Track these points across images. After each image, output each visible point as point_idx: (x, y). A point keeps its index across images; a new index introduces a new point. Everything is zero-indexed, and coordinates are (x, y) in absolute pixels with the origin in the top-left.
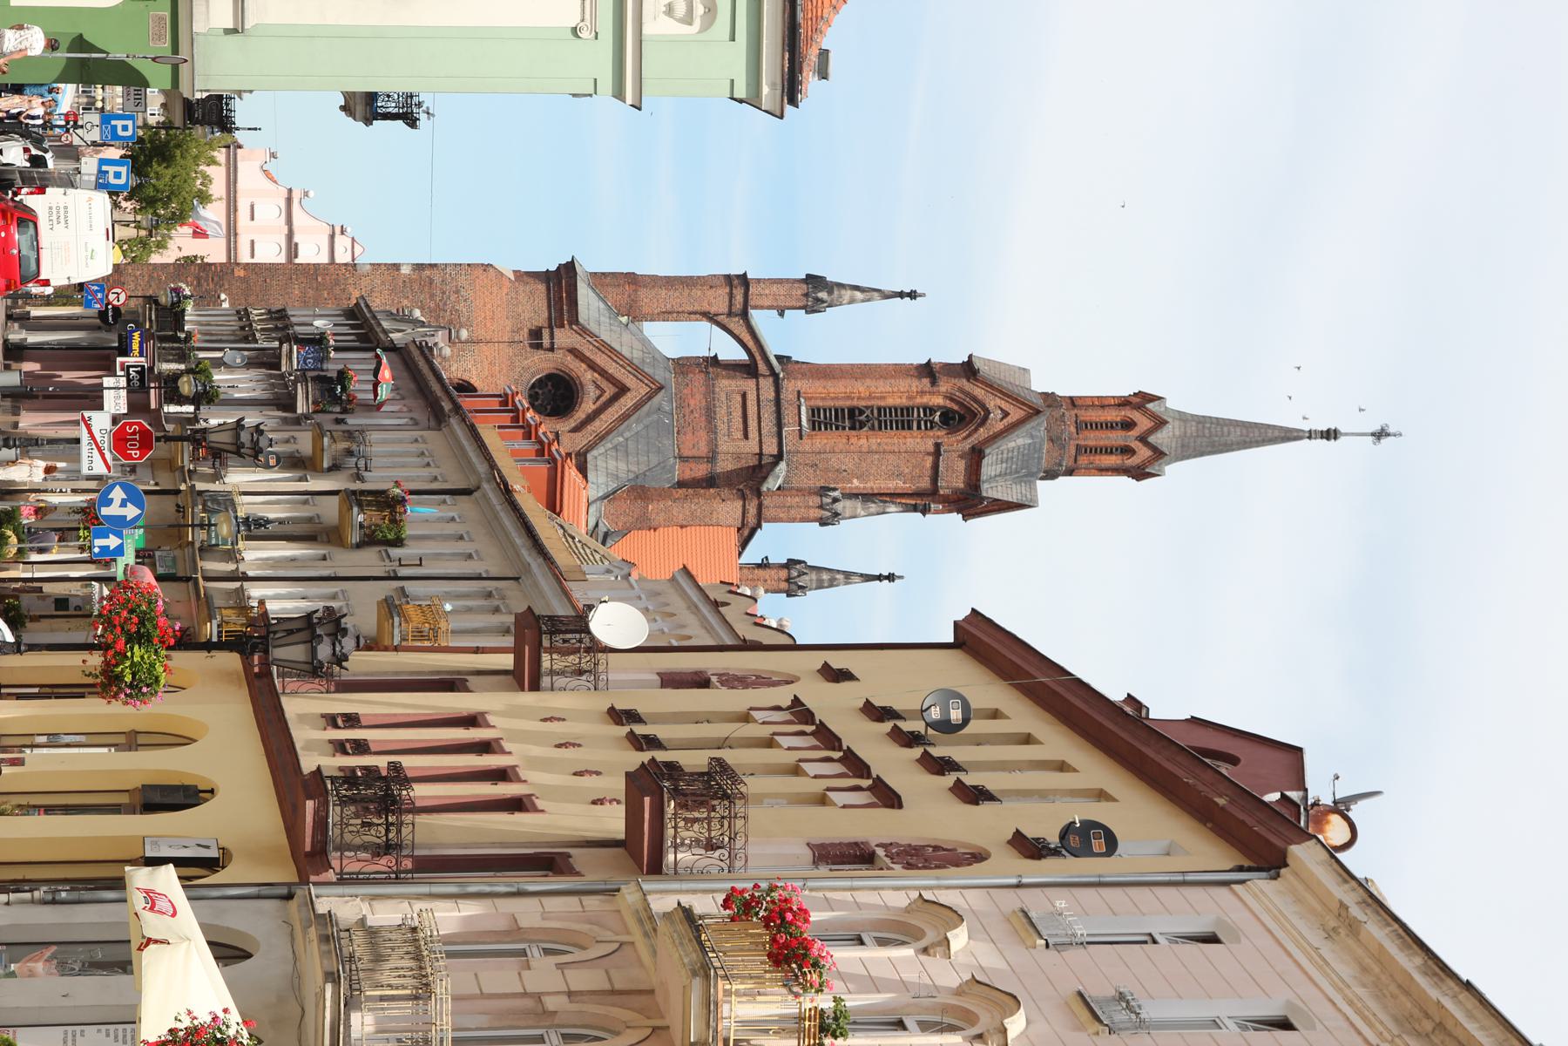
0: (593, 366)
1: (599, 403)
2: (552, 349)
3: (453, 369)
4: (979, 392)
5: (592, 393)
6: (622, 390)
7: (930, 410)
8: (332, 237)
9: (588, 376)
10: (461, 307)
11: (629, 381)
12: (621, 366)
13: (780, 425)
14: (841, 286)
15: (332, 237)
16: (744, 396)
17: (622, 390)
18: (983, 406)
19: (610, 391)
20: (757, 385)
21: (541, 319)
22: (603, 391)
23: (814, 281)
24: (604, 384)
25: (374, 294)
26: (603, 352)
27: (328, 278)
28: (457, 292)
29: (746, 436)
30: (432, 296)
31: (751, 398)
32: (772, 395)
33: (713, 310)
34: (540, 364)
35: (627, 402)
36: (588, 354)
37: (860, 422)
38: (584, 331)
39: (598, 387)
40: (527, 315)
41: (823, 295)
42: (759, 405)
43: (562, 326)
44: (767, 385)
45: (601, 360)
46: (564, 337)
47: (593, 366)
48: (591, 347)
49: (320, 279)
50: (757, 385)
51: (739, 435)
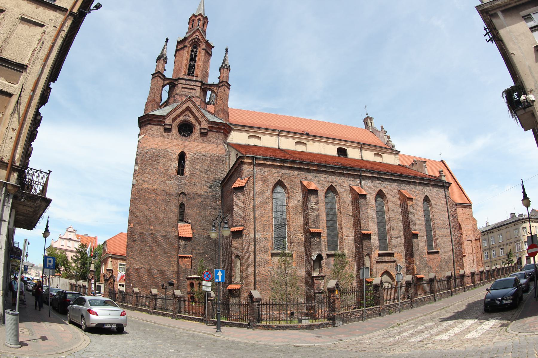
0: (179, 116)
1: (191, 116)
2: (171, 125)
3: (174, 157)
4: (190, 39)
5: (187, 118)
6: (188, 109)
7: (192, 51)
8: (68, 231)
9: (182, 118)
10: (152, 152)
11: (186, 106)
12: (180, 107)
13: (193, 81)
14: (162, 53)
15: (68, 231)
16: (183, 88)
17: (188, 109)
18: (194, 39)
19: (188, 112)
20: (180, 84)
21: (161, 129)
22: (187, 114)
23: (159, 59)
24: (185, 114)
25: (144, 180)
26: (175, 111)
27: (136, 195)
28: (147, 152)
29: (195, 89)
30: (147, 160)
31: (184, 86)
32: (184, 81)
33: (162, 84)
34: (175, 130)
35: (192, 107)
36: (175, 116)
37: (193, 65)
38: (168, 115)
39: (185, 116)
40: (158, 133)
41: (164, 56)
42: (186, 85)
43: (164, 122)
44: (180, 81)
45: (178, 112)
46: (168, 121)
47: (179, 116)
48: (173, 114)
49: (137, 197)
50: (180, 84)
51: (194, 91)
